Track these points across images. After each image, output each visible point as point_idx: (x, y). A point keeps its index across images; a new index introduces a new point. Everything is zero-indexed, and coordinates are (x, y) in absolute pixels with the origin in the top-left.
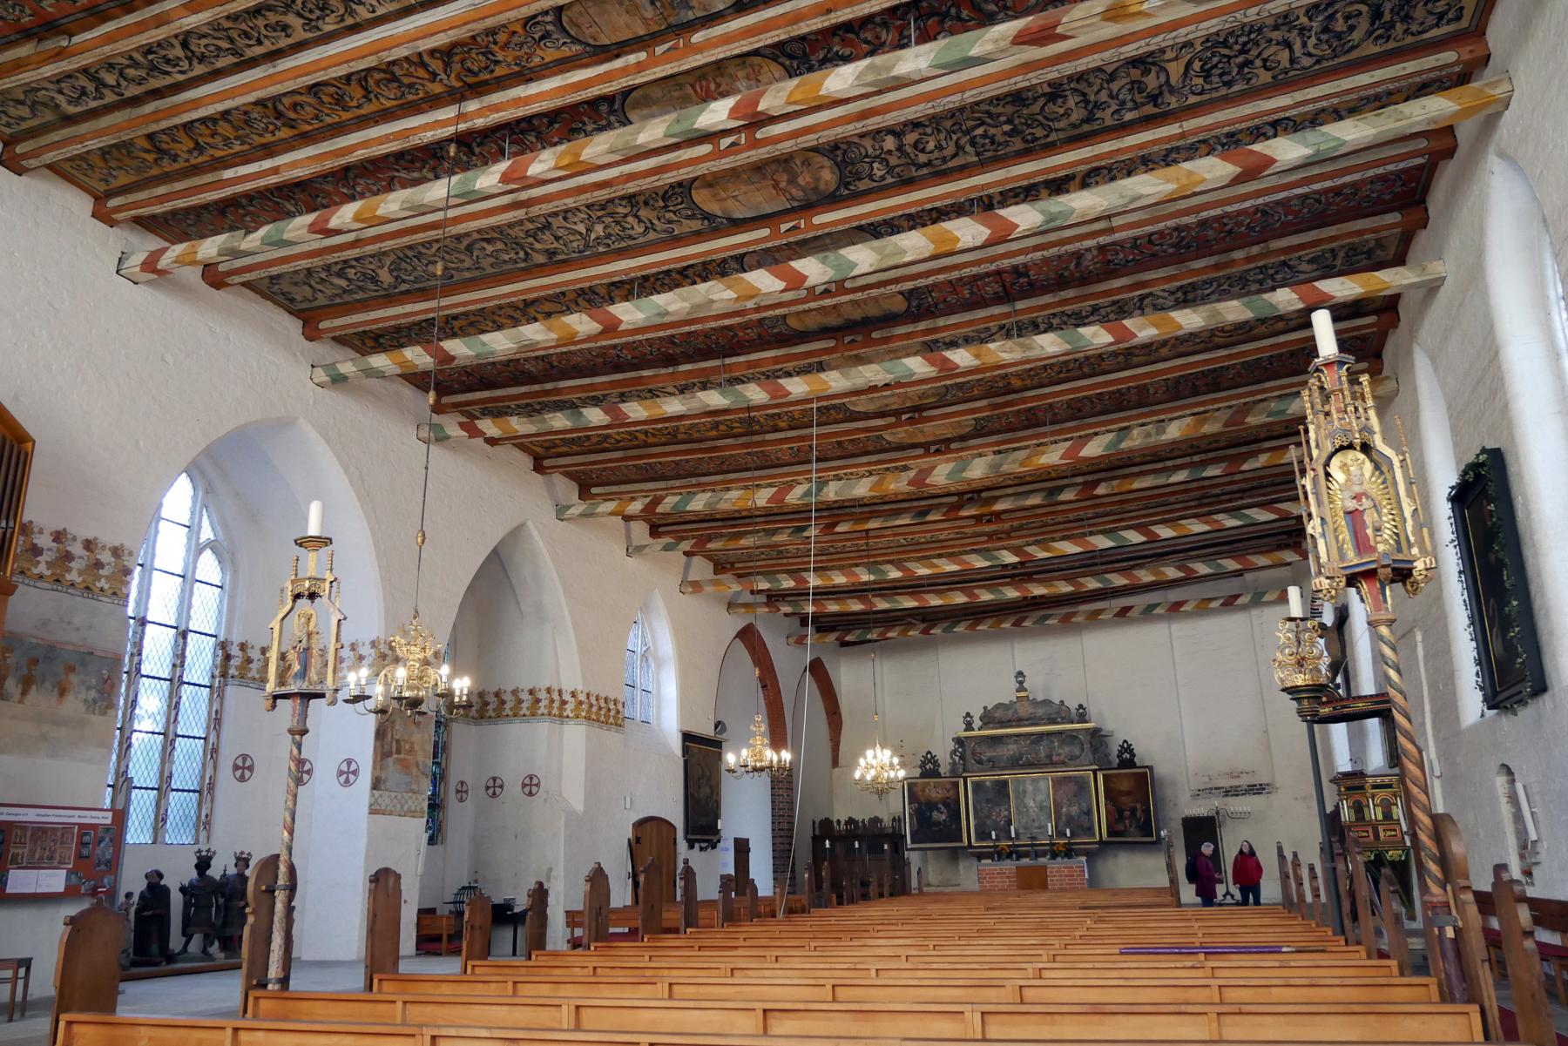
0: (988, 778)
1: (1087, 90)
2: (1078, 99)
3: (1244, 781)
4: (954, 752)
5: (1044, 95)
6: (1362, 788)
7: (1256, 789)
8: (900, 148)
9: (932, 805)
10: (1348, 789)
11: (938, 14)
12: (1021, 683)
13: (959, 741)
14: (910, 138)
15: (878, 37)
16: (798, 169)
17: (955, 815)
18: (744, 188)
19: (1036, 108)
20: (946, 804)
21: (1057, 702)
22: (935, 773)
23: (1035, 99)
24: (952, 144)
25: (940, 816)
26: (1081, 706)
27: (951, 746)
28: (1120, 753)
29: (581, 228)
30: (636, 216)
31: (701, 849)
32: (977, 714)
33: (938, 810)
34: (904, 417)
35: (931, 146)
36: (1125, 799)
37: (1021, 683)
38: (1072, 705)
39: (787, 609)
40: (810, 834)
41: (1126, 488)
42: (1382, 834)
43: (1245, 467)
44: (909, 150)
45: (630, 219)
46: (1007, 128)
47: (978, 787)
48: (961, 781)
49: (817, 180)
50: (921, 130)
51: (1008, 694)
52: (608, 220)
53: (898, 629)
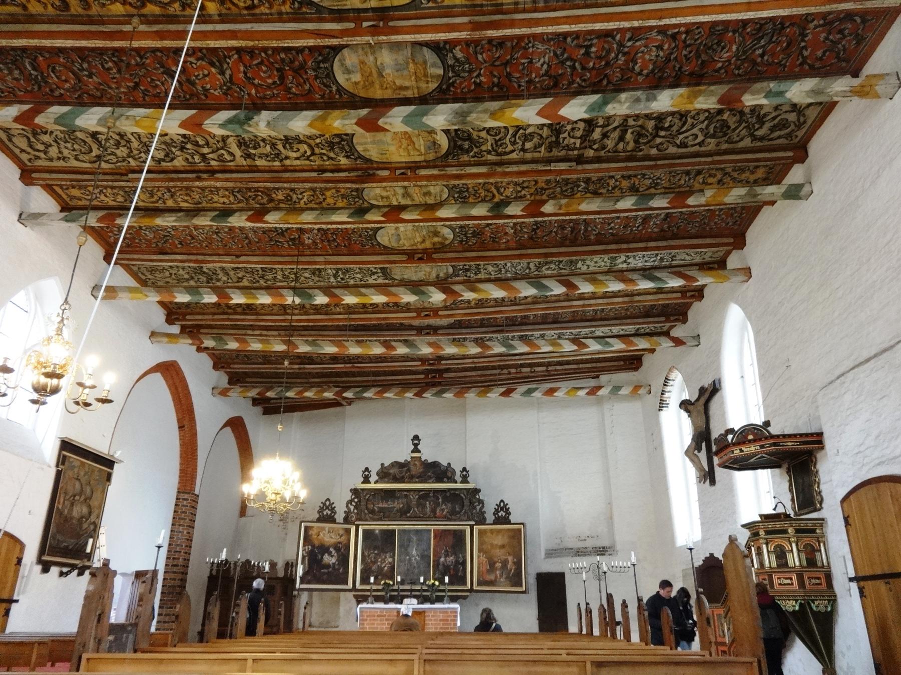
0: (377, 527)
3: (590, 544)
4: (350, 502)
6: (785, 531)
7: (602, 551)
9: (324, 549)
10: (768, 532)
12: (416, 445)
13: (355, 491)
20: (337, 549)
21: (445, 464)
22: (331, 519)
25: (330, 559)
26: (464, 469)
27: (348, 496)
28: (496, 512)
31: (62, 574)
32: (375, 469)
33: (330, 554)
34: (365, 24)
37: (416, 445)
39: (209, 343)
40: (207, 574)
41: (572, 209)
42: (807, 582)
43: (691, 201)
47: (368, 534)
51: (404, 454)
53: (315, 390)
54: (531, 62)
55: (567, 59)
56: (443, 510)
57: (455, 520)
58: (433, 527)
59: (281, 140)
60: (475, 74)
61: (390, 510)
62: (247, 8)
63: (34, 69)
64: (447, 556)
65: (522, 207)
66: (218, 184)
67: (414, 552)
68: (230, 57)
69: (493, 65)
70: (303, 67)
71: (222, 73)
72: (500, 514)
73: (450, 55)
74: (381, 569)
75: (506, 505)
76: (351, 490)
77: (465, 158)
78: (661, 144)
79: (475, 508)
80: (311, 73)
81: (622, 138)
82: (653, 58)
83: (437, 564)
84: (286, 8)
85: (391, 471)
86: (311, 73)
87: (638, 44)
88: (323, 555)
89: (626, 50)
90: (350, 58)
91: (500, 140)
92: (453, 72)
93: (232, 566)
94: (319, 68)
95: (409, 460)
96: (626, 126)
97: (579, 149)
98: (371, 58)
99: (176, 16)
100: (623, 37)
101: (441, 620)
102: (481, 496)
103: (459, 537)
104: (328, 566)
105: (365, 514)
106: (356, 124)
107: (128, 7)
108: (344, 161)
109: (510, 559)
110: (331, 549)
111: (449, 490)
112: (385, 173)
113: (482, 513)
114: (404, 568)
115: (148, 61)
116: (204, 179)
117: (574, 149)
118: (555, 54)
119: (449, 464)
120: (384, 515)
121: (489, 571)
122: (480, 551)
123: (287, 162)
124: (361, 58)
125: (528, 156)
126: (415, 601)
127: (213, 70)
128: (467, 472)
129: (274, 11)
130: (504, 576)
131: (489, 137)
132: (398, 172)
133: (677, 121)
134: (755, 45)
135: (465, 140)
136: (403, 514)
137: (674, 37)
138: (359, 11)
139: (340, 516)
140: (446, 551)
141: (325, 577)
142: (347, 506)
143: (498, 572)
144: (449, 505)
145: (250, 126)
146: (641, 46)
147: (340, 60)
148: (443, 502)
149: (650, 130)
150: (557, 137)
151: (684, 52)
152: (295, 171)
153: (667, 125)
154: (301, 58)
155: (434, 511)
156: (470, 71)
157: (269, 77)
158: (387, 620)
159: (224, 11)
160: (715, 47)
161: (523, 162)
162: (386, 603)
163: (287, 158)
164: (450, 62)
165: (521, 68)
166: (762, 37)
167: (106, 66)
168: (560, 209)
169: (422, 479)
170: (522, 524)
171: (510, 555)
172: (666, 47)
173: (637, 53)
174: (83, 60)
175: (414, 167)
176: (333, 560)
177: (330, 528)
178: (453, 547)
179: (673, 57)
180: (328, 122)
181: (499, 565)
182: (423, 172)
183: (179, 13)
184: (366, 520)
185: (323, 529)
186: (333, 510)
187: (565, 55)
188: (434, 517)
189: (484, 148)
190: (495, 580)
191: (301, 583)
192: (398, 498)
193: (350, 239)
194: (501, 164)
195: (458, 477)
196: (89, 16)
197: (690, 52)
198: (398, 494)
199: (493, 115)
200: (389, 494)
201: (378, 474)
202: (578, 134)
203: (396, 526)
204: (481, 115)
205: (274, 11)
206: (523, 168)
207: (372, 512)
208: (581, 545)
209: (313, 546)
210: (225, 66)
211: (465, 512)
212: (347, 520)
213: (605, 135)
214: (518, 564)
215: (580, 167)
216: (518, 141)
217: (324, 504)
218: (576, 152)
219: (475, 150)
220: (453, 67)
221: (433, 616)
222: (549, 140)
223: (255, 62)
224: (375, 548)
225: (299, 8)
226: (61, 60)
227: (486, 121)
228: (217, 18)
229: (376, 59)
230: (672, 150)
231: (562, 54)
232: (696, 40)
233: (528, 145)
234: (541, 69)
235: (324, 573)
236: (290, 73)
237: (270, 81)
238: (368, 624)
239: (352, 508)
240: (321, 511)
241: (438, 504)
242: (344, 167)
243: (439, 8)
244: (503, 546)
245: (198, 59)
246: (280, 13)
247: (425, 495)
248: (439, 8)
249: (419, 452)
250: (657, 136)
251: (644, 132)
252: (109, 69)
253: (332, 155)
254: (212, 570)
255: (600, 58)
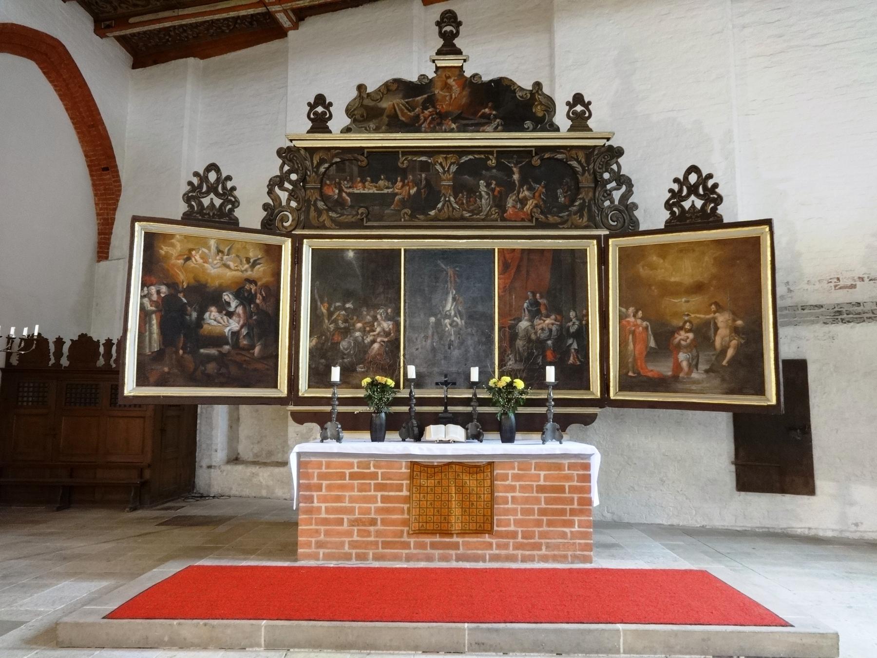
0: (351, 244)
4: (276, 182)
9: (207, 296)
13: (287, 154)
17: (264, 324)
21: (527, 85)
26: (578, 99)
27: (274, 167)
28: (675, 199)
32: (341, 99)
33: (223, 307)
36: (681, 303)
38: (561, 98)
48: (287, 247)
51: (417, 62)
56: (523, 202)
57: (554, 226)
58: (498, 243)
61: (385, 200)
64: (535, 313)
67: (449, 306)
72: (687, 205)
74: (362, 349)
75: (704, 180)
76: (280, 152)
79: (609, 195)
83: (510, 335)
85: (385, 104)
88: (202, 312)
93: (52, 348)
95: (431, 75)
101: (541, 489)
102: (626, 165)
103: (568, 267)
104: (218, 340)
105: (319, 212)
109: (722, 319)
110: (227, 297)
111: (541, 149)
113: (627, 209)
114: (424, 344)
119: (538, 85)
120: (368, 214)
121: (652, 355)
122: (624, 302)
126: (457, 432)
128: (587, 105)
130: (703, 367)
136: (421, 209)
139: (250, 214)
140: (536, 303)
141: (211, 367)
142: (270, 192)
143: (682, 356)
144: (540, 188)
148: (524, 181)
155: (499, 203)
158: (380, 487)
162: (377, 437)
169: (466, 119)
170: (768, 222)
171: (720, 308)
176: (234, 325)
177: (220, 241)
178: (551, 294)
181: (684, 337)
184: (324, 227)
185: (203, 242)
186: (229, 196)
188: (500, 218)
190: (675, 378)
191: (141, 380)
192: (404, 173)
195: (561, 119)
198: (403, 162)
200: (382, 162)
201: (349, 112)
203: (401, 242)
207: (339, 203)
208: (841, 297)
209: (173, 286)
211: (582, 208)
212: (269, 226)
214: (752, 336)
217: (203, 179)
221: (516, 477)
224: (348, 295)
235: (209, 358)
238: (324, 499)
239: (283, 196)
240: (193, 194)
241: (509, 187)
244: (698, 288)
247: (473, 163)
249: (459, 52)
254: (9, 355)
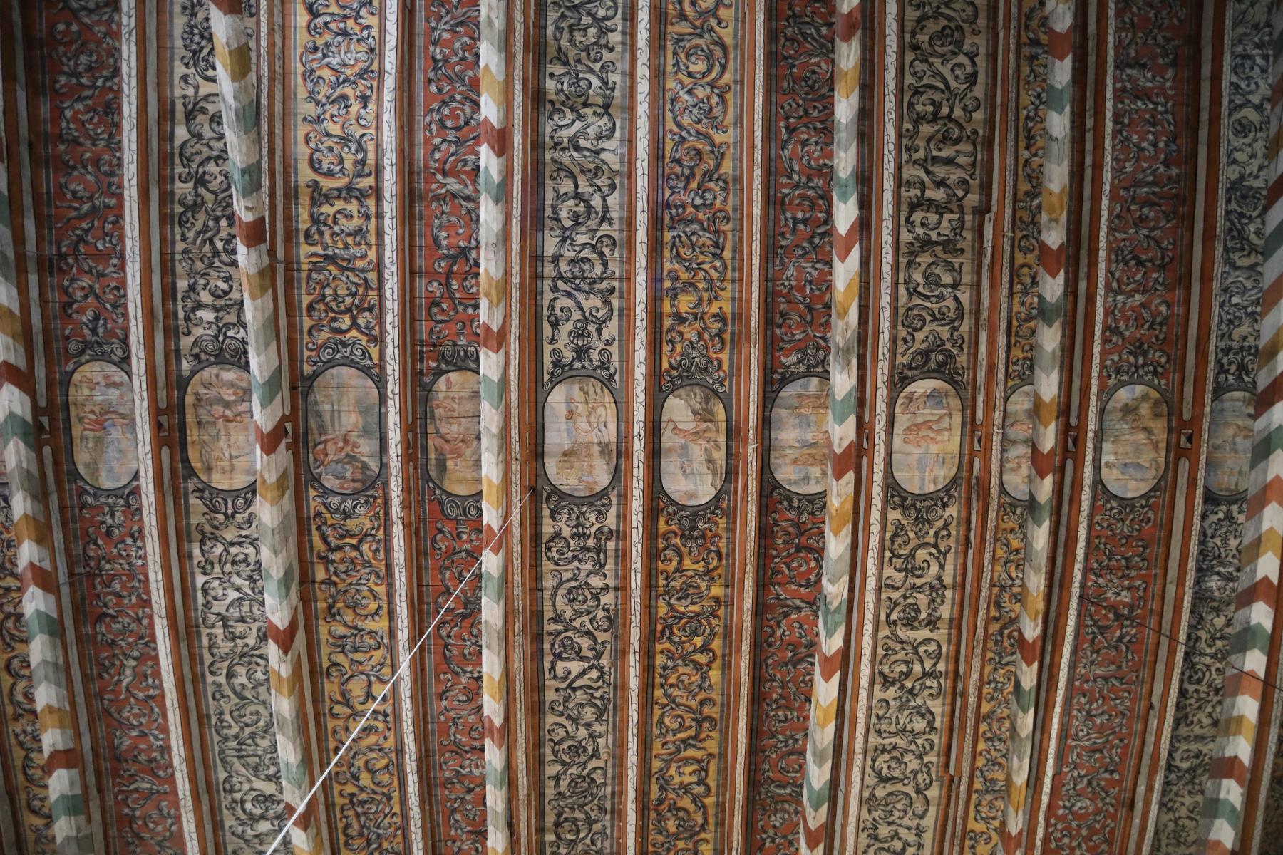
1: (204, 156)
2: (212, 163)
5: (195, 188)
8: (217, 310)
11: (77, 243)
14: (205, 297)
15: (83, 288)
16: (213, 393)
18: (222, 443)
19: (209, 197)
23: (197, 195)
24: (225, 268)
29: (233, 595)
30: (232, 544)
35: (224, 286)
44: (221, 302)
45: (233, 550)
46: (223, 223)
49: (232, 385)
50: (200, 288)
52: (228, 567)
54: (811, 282)
55: (811, 242)
59: (906, 577)
60: (822, 343)
62: (720, 558)
63: (784, 787)
65: (1048, 277)
66: (975, 676)
68: (778, 595)
69: (811, 324)
70: (797, 525)
71: (799, 609)
73: (792, 369)
77: (962, 360)
78: (964, 109)
80: (804, 518)
81: (949, 161)
82: (819, 148)
84: (722, 523)
86: (804, 518)
87: (796, 168)
89: (804, 179)
90: (786, 473)
91: (933, 315)
92: (817, 366)
94: (798, 508)
96: (925, 160)
97: (962, 212)
98: (788, 451)
99: (725, 626)
100: (785, 186)
106: (837, 480)
107: (714, 666)
108: (952, 511)
112: (977, 464)
115: (778, 676)
116: (966, 688)
117: (962, 221)
118: (802, 256)
123: (948, 580)
124: (788, 461)
125: (967, 278)
127: (794, 616)
129: (724, 535)
131: (927, 328)
132: (977, 447)
133: (925, 97)
134: (814, 39)
135: (928, 359)
137: (791, 131)
138: (728, 454)
145: (831, 603)
146: (801, 165)
147: (790, 484)
149: (936, 128)
150: (937, 243)
151: (815, 114)
152: (964, 575)
153: (930, 109)
154: (784, 524)
156: (818, 348)
157: (808, 562)
159: (722, 580)
160: (810, 83)
161: (978, 284)
163: (939, 578)
164: (802, 368)
165: (817, 292)
166: (804, 35)
167: (782, 718)
168: (1057, 221)
172: (805, 136)
173: (810, 167)
174: (773, 736)
175: (970, 425)
179: (819, 125)
180: (834, 513)
182: (980, 414)
183: (722, 623)
187: (805, 244)
189: (945, 335)
193: (1127, 537)
194: (977, 314)
196: (722, 705)
197: (815, 107)
199: (843, 314)
202: (933, 218)
204: (839, 329)
205: (724, 535)
206: (986, 283)
210: (789, 602)
213: (940, 184)
215: (994, 209)
216: (937, 293)
218: (968, 218)
219: (948, 346)
220: (809, 367)
222: (941, 254)
223: (786, 571)
225: (723, 510)
226: (774, 756)
227: (847, 324)
228: (729, 590)
229: (790, 447)
230: (979, 91)
231: (804, 248)
232: (799, 105)
233: (947, 279)
234: (822, 270)
236: (803, 539)
237: (813, 564)
242: (963, 515)
243: (731, 377)
245: (779, 627)
246: (727, 529)
248: (731, 377)
250: (949, 117)
251: (940, 136)
252: (786, 717)
253: (940, 523)
255: (812, 208)
